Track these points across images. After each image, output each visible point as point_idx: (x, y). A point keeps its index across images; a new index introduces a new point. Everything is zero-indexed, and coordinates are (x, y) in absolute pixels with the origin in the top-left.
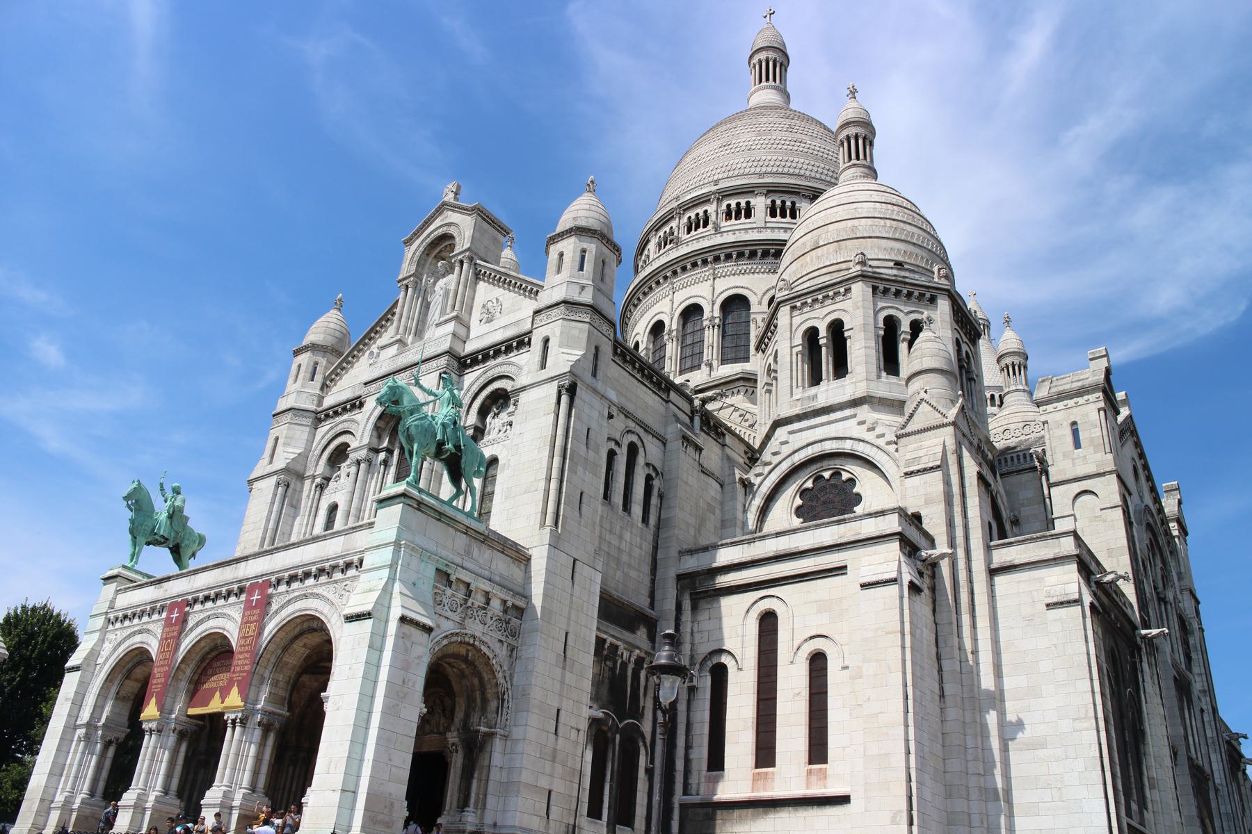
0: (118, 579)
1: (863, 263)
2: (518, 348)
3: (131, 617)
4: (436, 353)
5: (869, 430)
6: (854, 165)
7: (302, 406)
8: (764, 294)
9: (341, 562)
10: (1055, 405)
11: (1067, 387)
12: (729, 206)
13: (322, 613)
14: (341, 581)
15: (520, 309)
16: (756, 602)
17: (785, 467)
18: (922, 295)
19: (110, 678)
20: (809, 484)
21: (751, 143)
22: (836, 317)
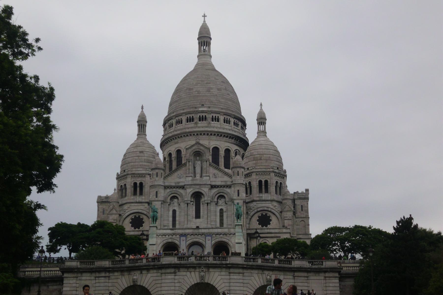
1: (273, 168)
2: (226, 187)
4: (207, 184)
5: (274, 207)
6: (263, 132)
8: (223, 148)
9: (230, 233)
10: (298, 200)
11: (301, 197)
12: (213, 116)
14: (230, 236)
15: (224, 178)
16: (263, 240)
17: (256, 211)
18: (282, 177)
19: (161, 248)
20: (260, 215)
21: (217, 93)
22: (267, 179)
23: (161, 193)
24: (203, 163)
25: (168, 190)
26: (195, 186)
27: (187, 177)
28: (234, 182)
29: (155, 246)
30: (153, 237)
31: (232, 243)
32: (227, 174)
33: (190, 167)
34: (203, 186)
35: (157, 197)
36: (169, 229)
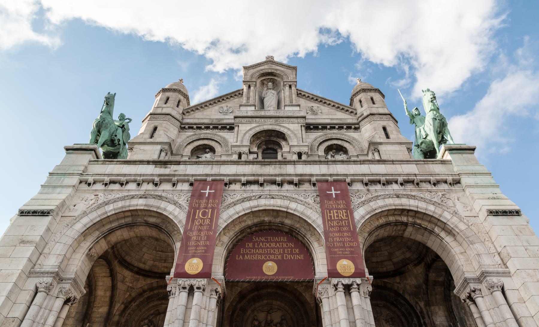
0: (93, 152)
2: (345, 129)
3: (125, 183)
7: (175, 116)
9: (432, 179)
13: (426, 209)
19: (85, 234)
23: (165, 129)
24: (283, 91)
25: (190, 133)
26: (263, 120)
27: (241, 108)
28: (365, 114)
29: (46, 220)
30: (55, 187)
31: (461, 219)
32: (343, 109)
33: (252, 94)
34: (284, 119)
35: (152, 137)
36: (148, 162)
